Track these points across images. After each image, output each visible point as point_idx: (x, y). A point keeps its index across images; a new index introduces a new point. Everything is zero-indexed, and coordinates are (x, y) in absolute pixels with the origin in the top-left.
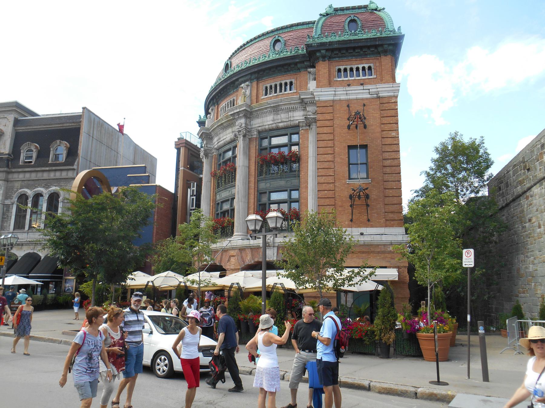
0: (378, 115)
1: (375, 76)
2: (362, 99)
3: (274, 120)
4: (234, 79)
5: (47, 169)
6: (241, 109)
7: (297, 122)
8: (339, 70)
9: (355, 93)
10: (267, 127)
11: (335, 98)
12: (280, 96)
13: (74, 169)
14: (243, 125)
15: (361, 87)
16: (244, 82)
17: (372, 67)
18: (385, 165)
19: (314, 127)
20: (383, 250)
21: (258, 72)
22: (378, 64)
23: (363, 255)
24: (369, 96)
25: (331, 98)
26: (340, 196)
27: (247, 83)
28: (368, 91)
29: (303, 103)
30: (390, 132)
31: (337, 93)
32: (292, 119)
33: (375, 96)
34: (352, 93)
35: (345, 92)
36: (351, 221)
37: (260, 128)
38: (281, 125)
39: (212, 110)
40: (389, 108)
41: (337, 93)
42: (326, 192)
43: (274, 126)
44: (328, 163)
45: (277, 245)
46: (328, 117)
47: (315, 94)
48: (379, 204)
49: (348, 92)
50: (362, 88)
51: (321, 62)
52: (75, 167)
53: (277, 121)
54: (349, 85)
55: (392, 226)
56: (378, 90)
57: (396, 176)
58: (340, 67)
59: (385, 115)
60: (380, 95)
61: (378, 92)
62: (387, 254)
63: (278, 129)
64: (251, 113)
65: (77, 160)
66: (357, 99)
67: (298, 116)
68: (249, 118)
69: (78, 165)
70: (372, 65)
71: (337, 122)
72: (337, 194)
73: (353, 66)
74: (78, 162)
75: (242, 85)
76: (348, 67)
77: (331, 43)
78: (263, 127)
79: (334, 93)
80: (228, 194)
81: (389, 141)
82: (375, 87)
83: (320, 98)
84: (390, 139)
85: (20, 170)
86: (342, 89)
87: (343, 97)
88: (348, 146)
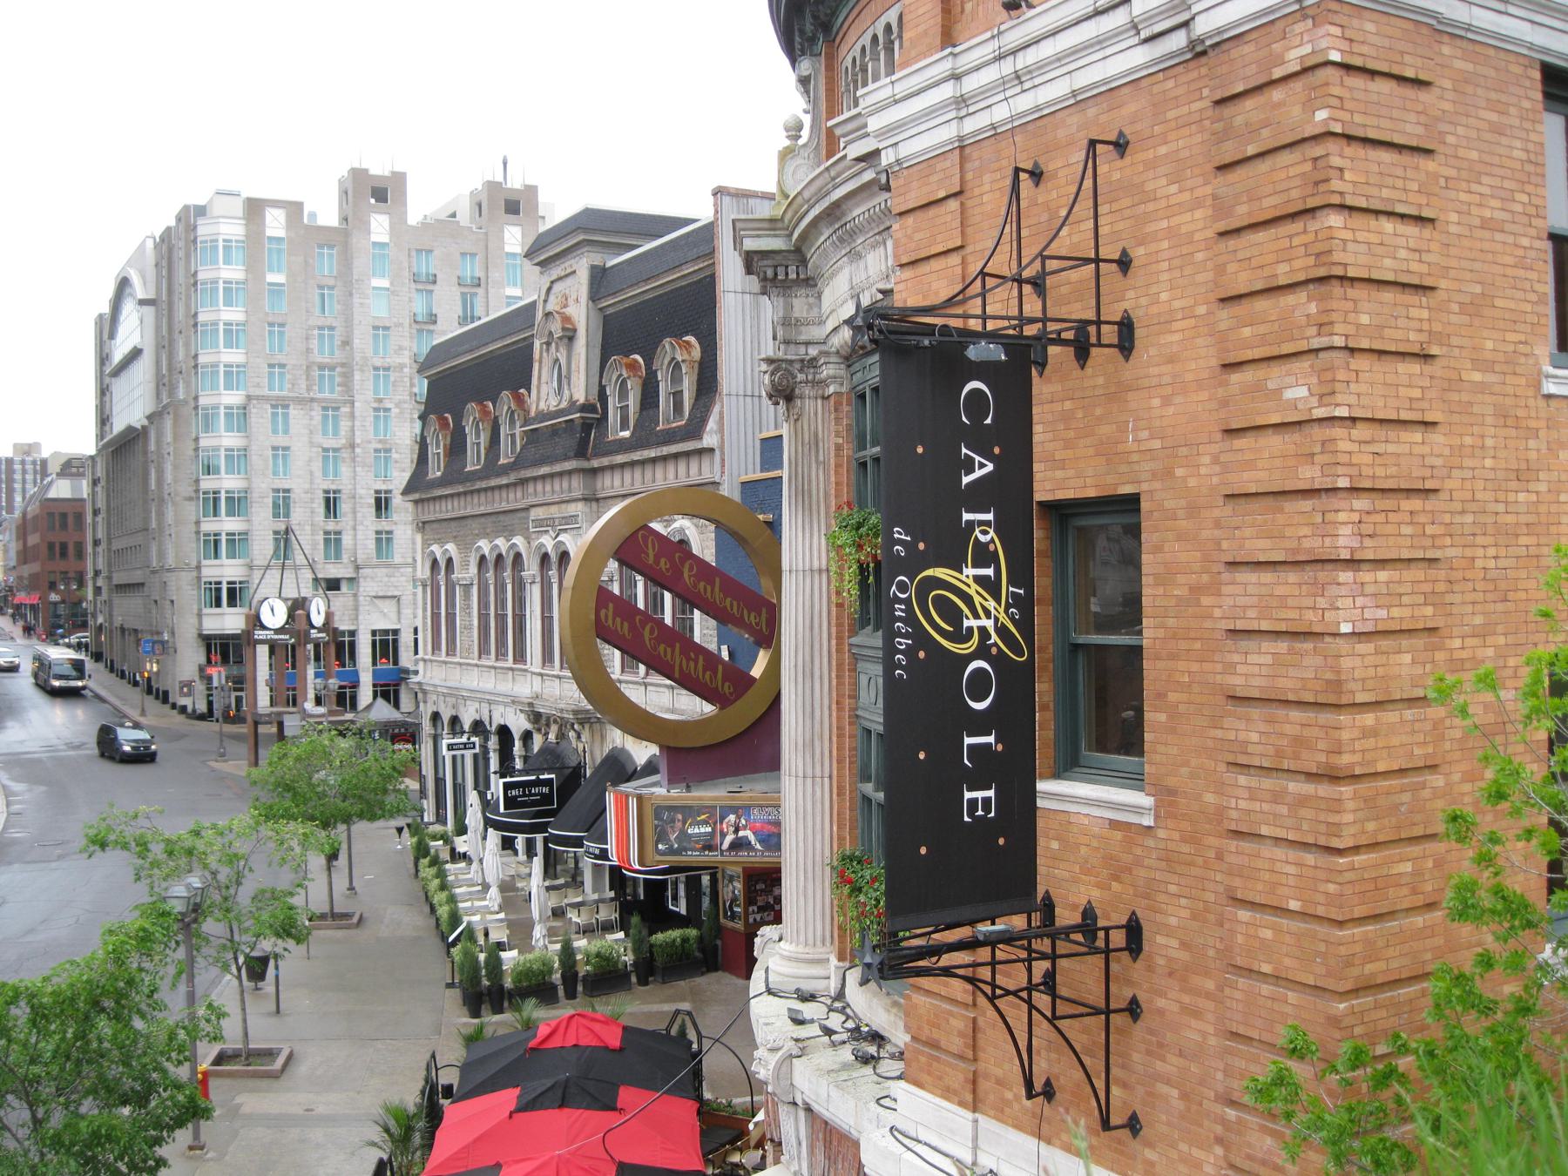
0: (1198, 223)
5: (652, 453)
9: (1059, 59)
11: (970, 126)
13: (712, 450)
18: (1237, 682)
24: (1140, 56)
25: (947, 133)
30: (1274, 376)
33: (1178, 40)
34: (1041, 66)
40: (1267, 139)
41: (971, 84)
48: (1197, 1014)
52: (709, 440)
57: (1303, 801)
59: (1243, 213)
60: (1202, 26)
64: (799, 254)
65: (716, 409)
68: (809, 282)
69: (721, 430)
74: (721, 418)
79: (947, 91)
81: (1266, 462)
84: (1274, 441)
85: (620, 459)
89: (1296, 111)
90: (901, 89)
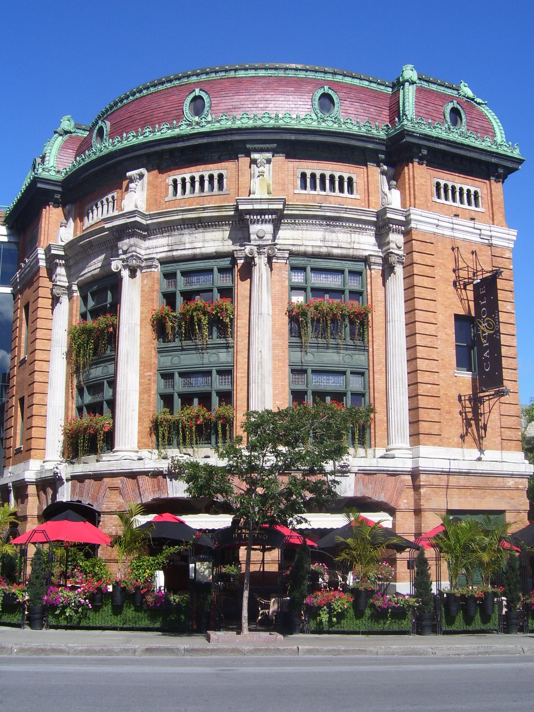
1: (483, 210)
2: (470, 241)
3: (324, 240)
6: (271, 207)
7: (366, 253)
8: (438, 184)
10: (310, 250)
12: (331, 199)
14: (269, 236)
15: (471, 223)
17: (480, 194)
19: (399, 269)
20: (502, 485)
22: (485, 192)
23: (479, 491)
24: (477, 239)
26: (446, 394)
27: (269, 155)
28: (478, 232)
29: (382, 226)
31: (441, 223)
32: (356, 246)
35: (451, 226)
36: (462, 437)
37: (294, 249)
38: (336, 251)
42: (429, 386)
43: (324, 250)
44: (429, 339)
45: (355, 469)
46: (428, 260)
47: (412, 217)
49: (455, 226)
50: (472, 225)
51: (416, 164)
53: (330, 244)
54: (456, 216)
55: (509, 449)
56: (493, 234)
57: (512, 373)
58: (439, 180)
61: (491, 237)
62: (505, 492)
63: (329, 256)
66: (464, 240)
67: (365, 243)
70: (478, 190)
71: (438, 272)
72: (442, 392)
73: (455, 185)
75: (255, 156)
76: (450, 184)
77: (438, 140)
78: (302, 249)
82: (488, 228)
83: (419, 227)
86: (447, 220)
87: (448, 233)
88: (455, 315)
89: (507, 264)
90: (423, 214)
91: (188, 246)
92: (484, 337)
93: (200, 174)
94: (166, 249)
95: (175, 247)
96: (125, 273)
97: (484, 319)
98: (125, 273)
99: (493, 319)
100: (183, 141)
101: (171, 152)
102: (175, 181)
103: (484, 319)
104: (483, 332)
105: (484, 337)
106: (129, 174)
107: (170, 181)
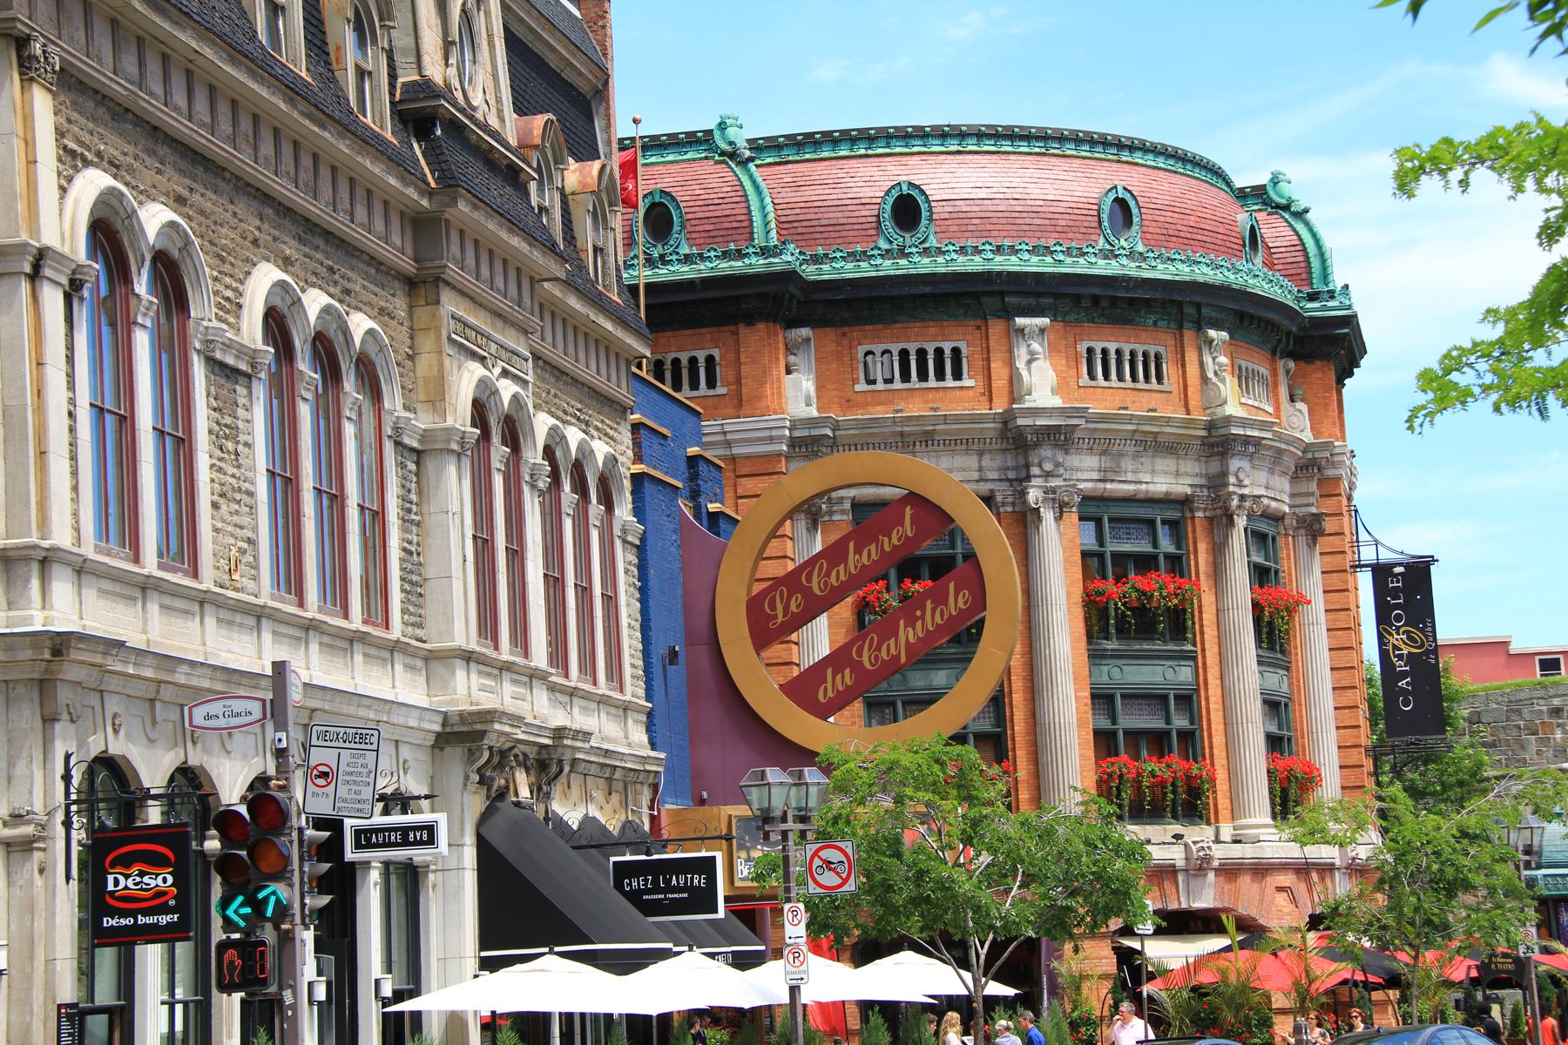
4: (1198, 299)
16: (1218, 326)
21: (1242, 316)
39: (1042, 331)
75: (1212, 333)
80: (1160, 679)
91: (1130, 477)
92: (1400, 657)
93: (1132, 346)
94: (1095, 476)
95: (1110, 476)
96: (1048, 516)
97: (1398, 628)
98: (1048, 516)
99: (1422, 631)
100: (1127, 289)
101: (1096, 299)
102: (1090, 351)
103: (1398, 628)
104: (1395, 647)
105: (1400, 657)
106: (1020, 321)
107: (1082, 348)
